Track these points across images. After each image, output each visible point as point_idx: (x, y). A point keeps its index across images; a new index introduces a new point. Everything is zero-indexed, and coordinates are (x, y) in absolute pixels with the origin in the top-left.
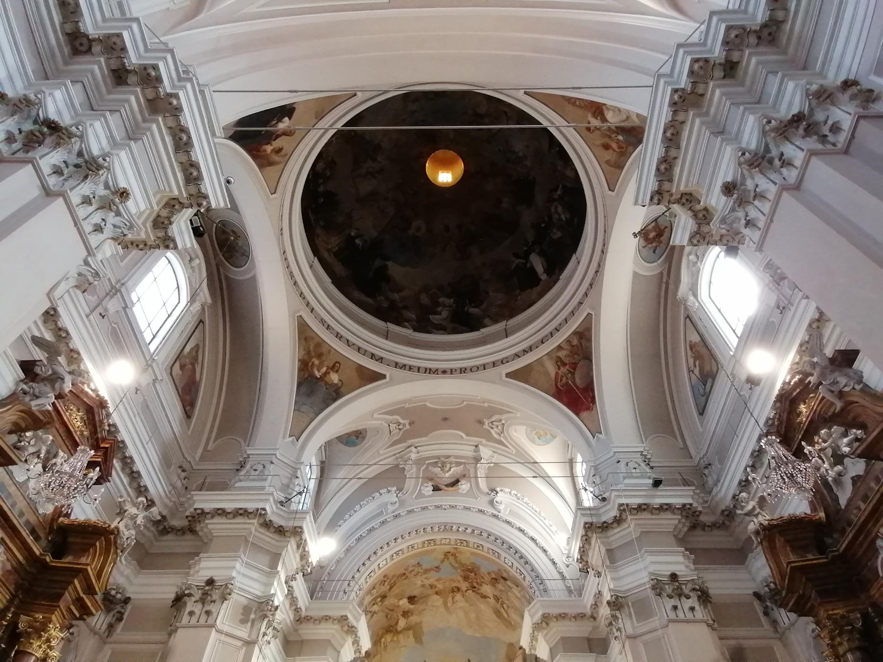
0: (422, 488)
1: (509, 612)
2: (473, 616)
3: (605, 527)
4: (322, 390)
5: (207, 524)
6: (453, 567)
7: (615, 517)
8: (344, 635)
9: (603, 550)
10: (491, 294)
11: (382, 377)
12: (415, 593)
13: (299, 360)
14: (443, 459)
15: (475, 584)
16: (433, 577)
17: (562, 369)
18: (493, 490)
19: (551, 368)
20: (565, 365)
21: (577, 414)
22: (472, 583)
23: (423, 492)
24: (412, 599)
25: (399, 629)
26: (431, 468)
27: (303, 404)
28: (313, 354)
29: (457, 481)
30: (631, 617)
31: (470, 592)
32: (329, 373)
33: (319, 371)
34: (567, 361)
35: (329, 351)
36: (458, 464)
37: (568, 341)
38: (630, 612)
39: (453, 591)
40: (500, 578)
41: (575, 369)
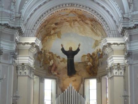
1: (97, 30)
3: (130, 28)
6: (74, 14)
7: (134, 26)
9: (128, 35)
12: (58, 22)
15: (83, 20)
16: (65, 17)
22: (82, 19)
25: (51, 34)
30: (132, 58)
31: (81, 21)
38: (132, 57)
39: (74, 21)
40: (93, 20)
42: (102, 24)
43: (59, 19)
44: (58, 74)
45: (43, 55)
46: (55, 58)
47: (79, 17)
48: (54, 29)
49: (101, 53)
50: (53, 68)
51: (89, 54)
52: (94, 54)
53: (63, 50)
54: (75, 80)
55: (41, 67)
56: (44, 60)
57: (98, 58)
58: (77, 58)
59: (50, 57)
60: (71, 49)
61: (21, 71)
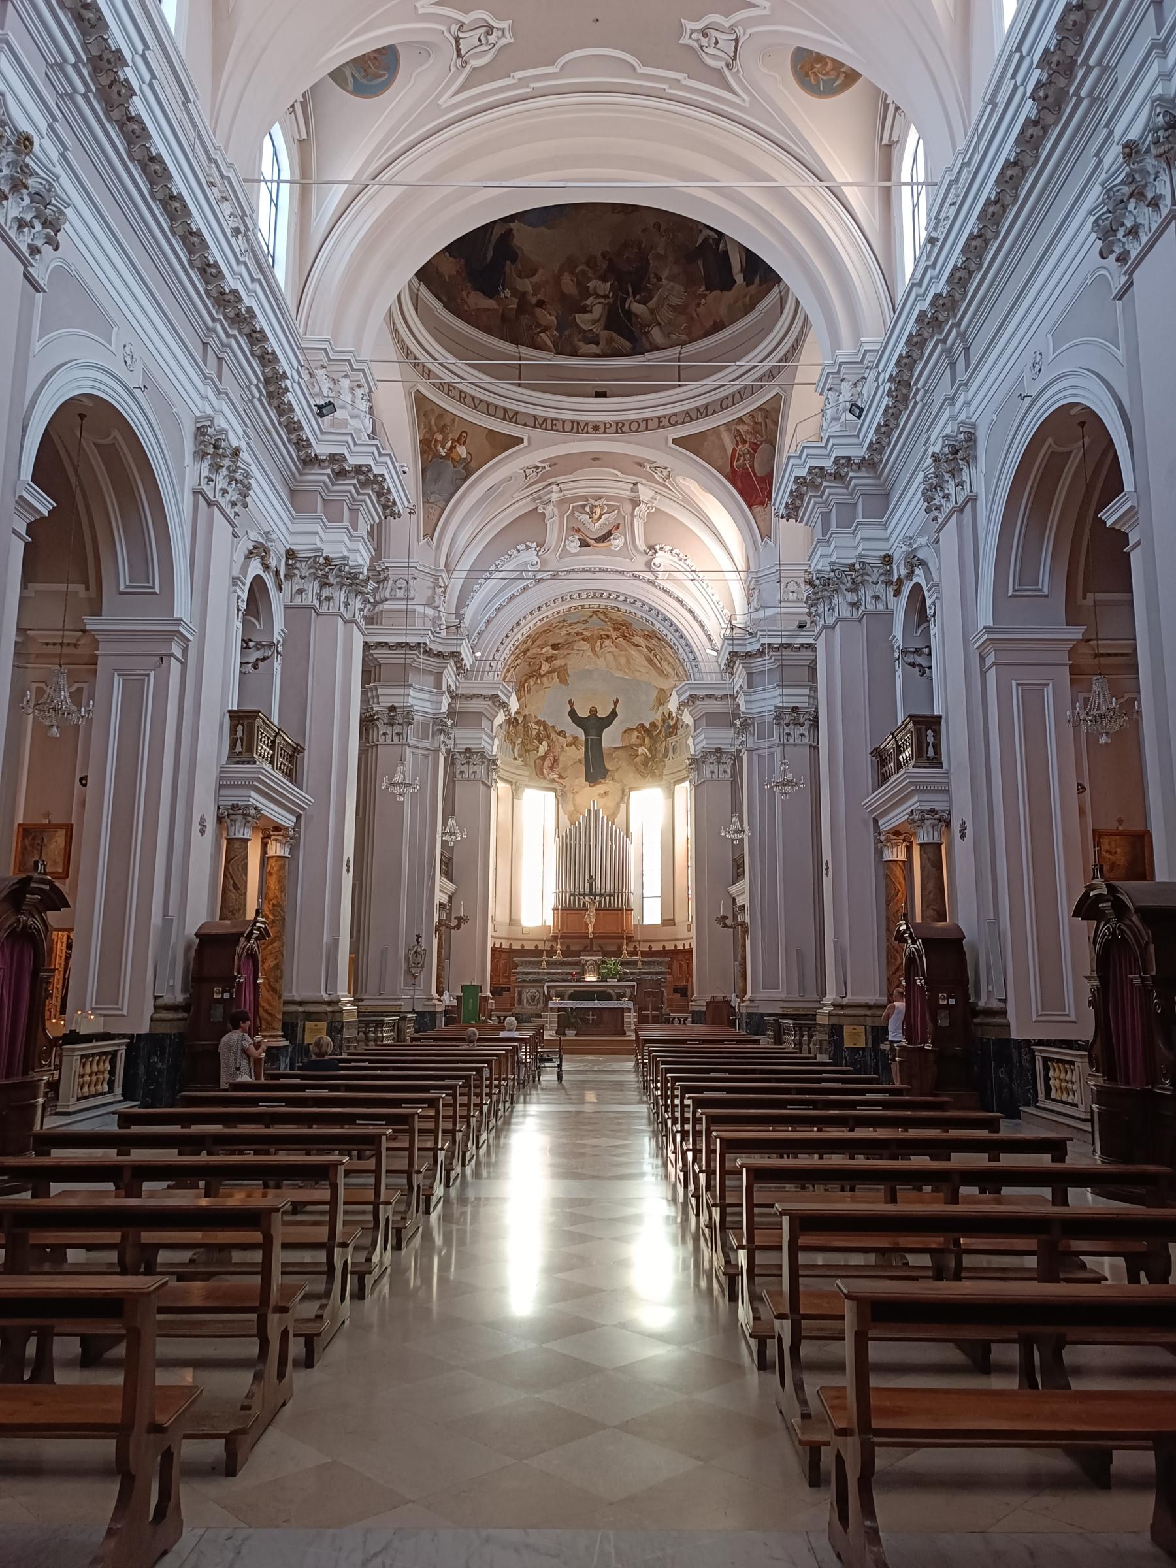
0: (567, 543)
2: (623, 660)
3: (749, 655)
4: (450, 469)
5: (372, 654)
8: (497, 709)
9: (745, 673)
10: (664, 281)
11: (521, 440)
13: (420, 442)
14: (592, 501)
17: (740, 446)
18: (651, 548)
19: (729, 443)
20: (744, 442)
21: (750, 506)
23: (568, 548)
24: (555, 647)
25: (542, 673)
26: (577, 514)
27: (431, 493)
28: (436, 429)
29: (609, 534)
30: (754, 735)
32: (455, 447)
33: (443, 448)
34: (748, 438)
35: (454, 420)
36: (611, 509)
37: (751, 415)
39: (602, 638)
40: (650, 635)
41: (755, 450)
42: (675, 644)
43: (563, 632)
44: (560, 777)
45: (520, 727)
46: (553, 735)
47: (615, 629)
48: (549, 659)
49: (672, 723)
50: (547, 763)
51: (643, 726)
52: (653, 725)
53: (573, 714)
54: (606, 793)
55: (515, 759)
56: (522, 742)
57: (666, 737)
58: (610, 737)
59: (539, 733)
60: (594, 711)
61: (464, 768)
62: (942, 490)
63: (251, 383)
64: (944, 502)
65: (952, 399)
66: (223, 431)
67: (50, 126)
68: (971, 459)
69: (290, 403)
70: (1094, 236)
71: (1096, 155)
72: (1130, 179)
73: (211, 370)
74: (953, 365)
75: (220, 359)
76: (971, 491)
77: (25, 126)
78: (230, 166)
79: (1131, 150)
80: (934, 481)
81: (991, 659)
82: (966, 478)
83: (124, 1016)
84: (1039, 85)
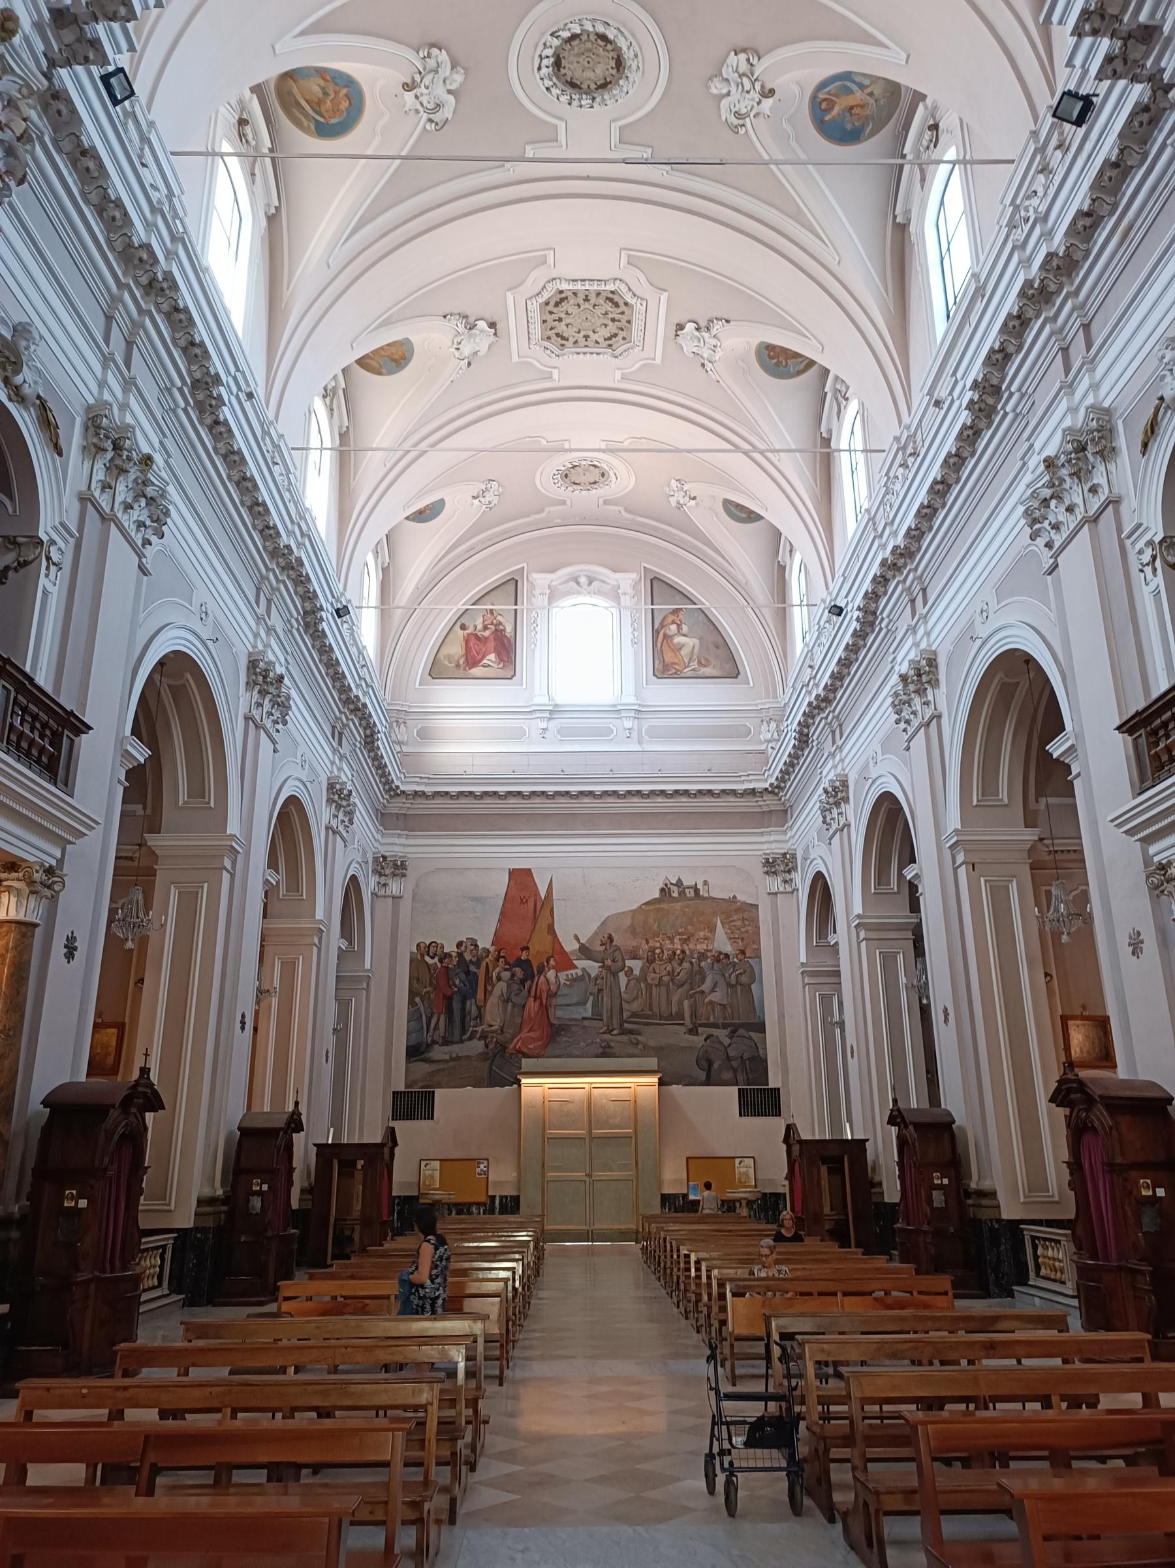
62: (910, 706)
63: (292, 616)
64: (912, 717)
65: (913, 629)
66: (270, 663)
67: (161, 443)
68: (935, 683)
69: (323, 630)
70: (1023, 521)
71: (1023, 458)
72: (1050, 485)
73: (261, 610)
74: (913, 601)
75: (269, 601)
76: (936, 709)
77: (146, 449)
78: (281, 436)
79: (1050, 463)
80: (905, 698)
81: (960, 858)
82: (930, 698)
83: (170, 1211)
84: (971, 401)
